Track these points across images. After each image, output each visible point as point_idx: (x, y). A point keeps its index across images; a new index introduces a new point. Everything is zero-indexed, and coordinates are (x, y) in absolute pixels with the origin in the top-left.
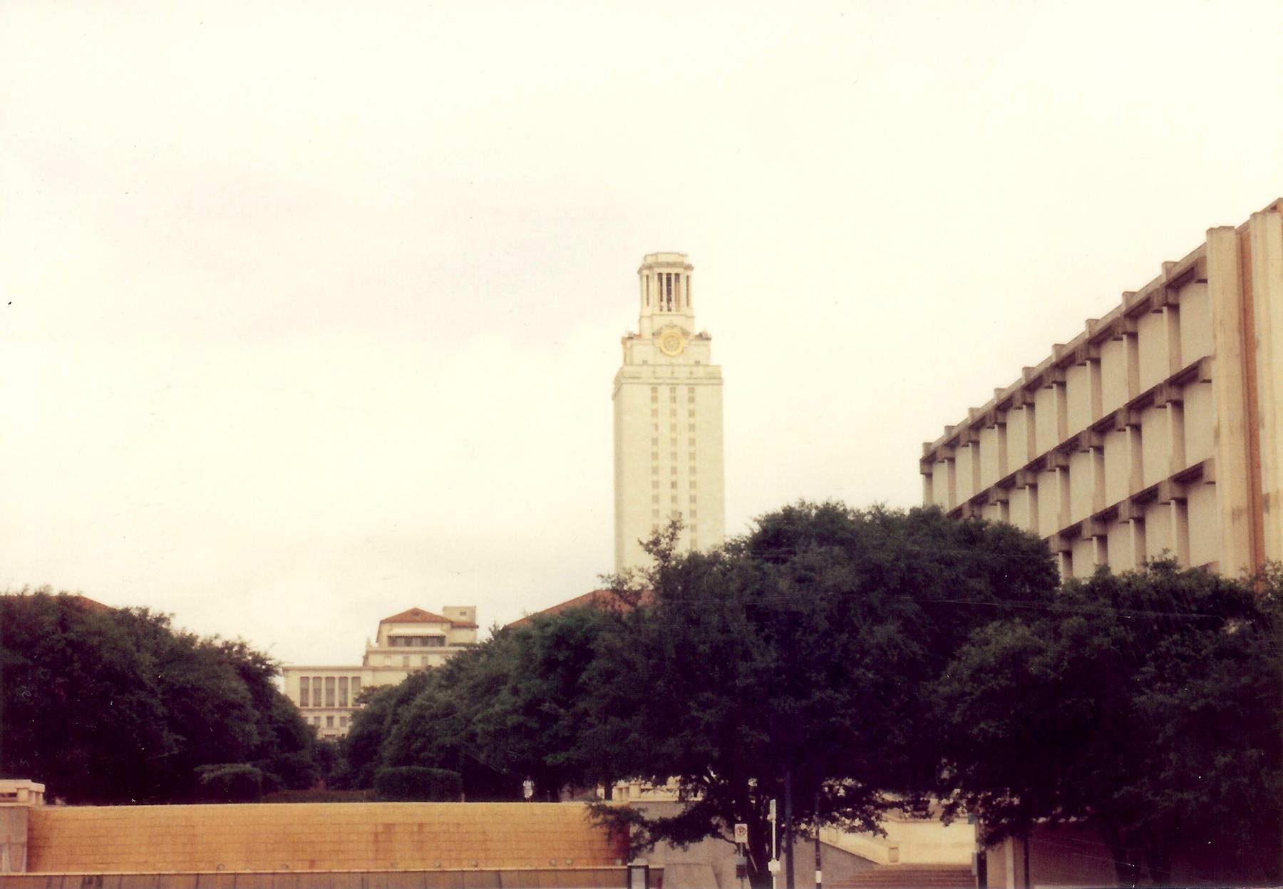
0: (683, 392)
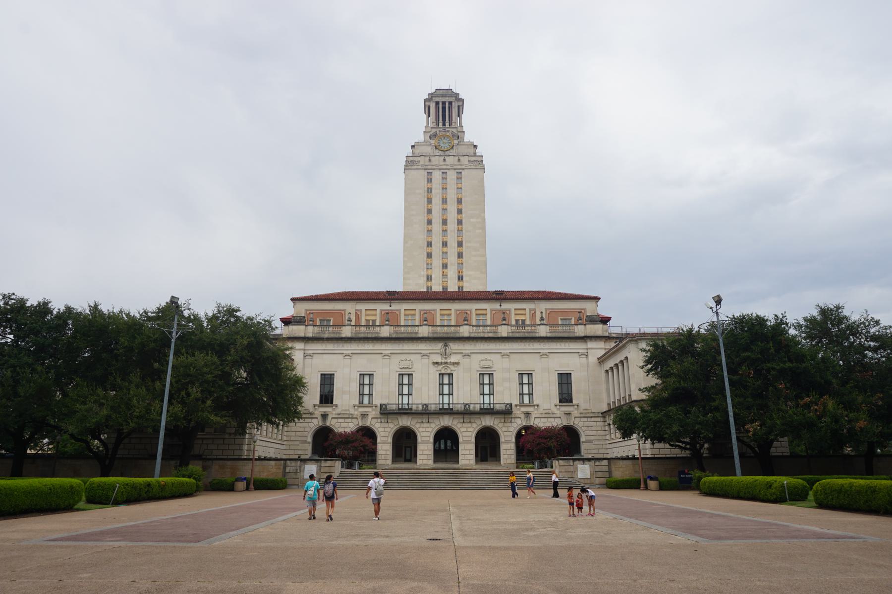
0: (452, 175)
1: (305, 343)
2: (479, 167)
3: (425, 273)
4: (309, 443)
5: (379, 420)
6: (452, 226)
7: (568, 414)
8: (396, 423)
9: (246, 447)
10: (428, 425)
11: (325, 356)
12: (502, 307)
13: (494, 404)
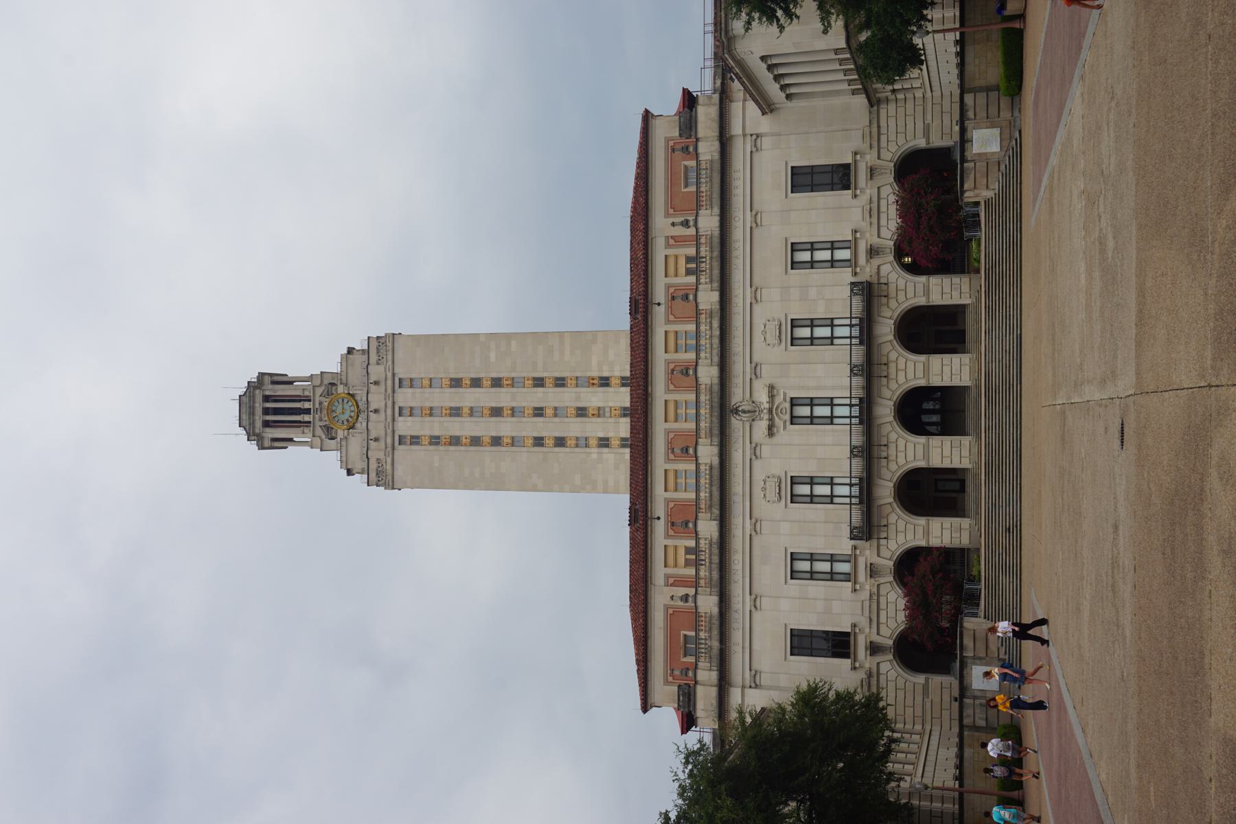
0: (405, 397)
1: (730, 685)
2: (390, 345)
3: (594, 452)
4: (927, 680)
5: (883, 542)
6: (503, 397)
7: (872, 172)
8: (888, 509)
9: (937, 805)
10: (892, 446)
11: (756, 647)
12: (662, 301)
13: (851, 318)
